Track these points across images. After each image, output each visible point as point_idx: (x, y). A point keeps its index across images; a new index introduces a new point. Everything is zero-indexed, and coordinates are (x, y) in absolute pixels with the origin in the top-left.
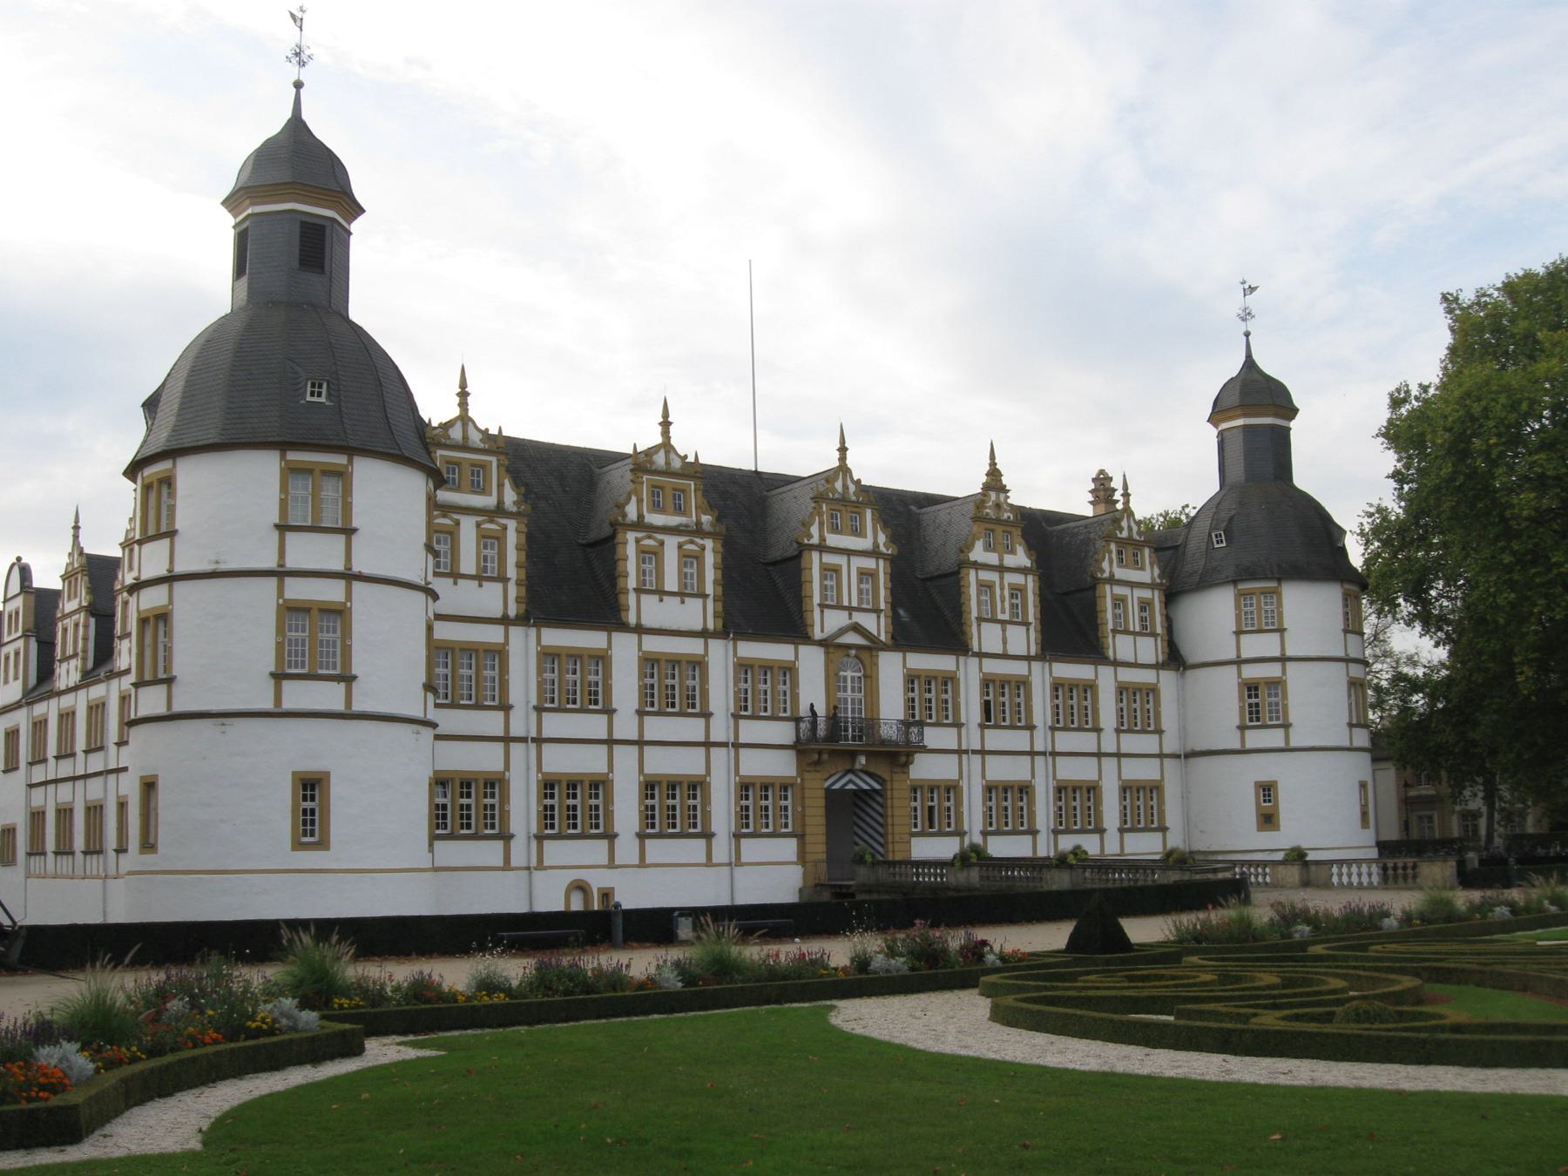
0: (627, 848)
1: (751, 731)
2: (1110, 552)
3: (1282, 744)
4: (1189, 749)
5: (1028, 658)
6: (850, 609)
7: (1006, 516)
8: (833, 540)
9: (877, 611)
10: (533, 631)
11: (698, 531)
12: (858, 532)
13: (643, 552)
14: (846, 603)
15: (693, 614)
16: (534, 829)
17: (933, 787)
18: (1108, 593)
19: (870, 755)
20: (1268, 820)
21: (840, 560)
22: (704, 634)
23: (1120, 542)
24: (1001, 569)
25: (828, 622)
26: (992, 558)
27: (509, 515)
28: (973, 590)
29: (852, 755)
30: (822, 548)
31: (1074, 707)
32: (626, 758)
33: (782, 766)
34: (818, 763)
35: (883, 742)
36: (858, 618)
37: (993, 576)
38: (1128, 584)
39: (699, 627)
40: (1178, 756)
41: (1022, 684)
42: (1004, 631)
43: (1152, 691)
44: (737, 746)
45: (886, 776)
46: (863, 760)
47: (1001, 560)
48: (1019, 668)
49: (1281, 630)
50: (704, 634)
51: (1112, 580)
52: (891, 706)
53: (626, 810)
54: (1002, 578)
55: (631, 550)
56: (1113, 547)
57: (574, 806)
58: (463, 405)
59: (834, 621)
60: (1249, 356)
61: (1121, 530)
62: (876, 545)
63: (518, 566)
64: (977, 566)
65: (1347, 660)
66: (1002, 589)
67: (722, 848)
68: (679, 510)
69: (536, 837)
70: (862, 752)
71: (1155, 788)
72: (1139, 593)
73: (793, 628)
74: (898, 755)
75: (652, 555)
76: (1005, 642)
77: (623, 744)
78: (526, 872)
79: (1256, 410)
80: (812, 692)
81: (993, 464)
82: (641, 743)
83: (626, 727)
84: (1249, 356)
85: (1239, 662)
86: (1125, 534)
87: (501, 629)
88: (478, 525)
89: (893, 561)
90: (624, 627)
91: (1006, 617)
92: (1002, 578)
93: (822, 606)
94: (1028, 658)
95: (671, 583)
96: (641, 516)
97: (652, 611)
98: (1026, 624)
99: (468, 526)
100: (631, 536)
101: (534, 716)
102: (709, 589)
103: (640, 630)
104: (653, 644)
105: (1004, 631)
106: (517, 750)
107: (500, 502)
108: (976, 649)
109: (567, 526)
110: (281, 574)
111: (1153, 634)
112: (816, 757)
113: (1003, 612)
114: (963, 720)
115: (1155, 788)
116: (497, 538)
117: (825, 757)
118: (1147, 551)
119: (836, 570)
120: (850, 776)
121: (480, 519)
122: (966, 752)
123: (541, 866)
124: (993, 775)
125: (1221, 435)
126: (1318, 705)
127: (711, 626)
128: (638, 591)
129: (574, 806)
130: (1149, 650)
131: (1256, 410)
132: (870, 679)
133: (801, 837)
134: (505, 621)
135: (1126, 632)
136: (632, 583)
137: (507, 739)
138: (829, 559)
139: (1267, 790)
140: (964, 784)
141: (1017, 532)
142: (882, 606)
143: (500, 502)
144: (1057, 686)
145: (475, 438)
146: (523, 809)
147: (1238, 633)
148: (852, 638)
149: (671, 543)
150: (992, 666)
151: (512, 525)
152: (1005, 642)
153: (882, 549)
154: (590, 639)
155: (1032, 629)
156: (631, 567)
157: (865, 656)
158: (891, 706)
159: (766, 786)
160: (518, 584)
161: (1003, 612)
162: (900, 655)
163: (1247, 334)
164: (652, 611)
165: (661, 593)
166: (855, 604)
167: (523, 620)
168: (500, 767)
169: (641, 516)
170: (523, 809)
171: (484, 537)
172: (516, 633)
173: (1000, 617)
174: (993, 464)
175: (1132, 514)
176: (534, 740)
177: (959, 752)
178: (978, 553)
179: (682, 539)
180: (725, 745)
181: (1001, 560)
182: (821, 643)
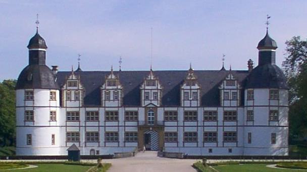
1: (128, 123)
2: (224, 83)
5: (197, 107)
8: (147, 88)
12: (154, 85)
15: (116, 104)
17: (171, 134)
20: (250, 141)
21: (149, 91)
23: (227, 80)
24: (191, 89)
25: (145, 103)
28: (182, 94)
31: (211, 117)
33: (135, 130)
35: (158, 125)
36: (153, 102)
37: (189, 91)
38: (229, 90)
39: (117, 106)
41: (196, 113)
43: (235, 113)
46: (151, 129)
48: (195, 109)
49: (253, 100)
52: (160, 117)
53: (102, 137)
55: (104, 93)
56: (225, 82)
59: (147, 102)
60: (267, 33)
61: (228, 77)
64: (184, 89)
65: (269, 106)
67: (200, 144)
68: (114, 85)
71: (235, 134)
72: (232, 91)
73: (138, 104)
74: (163, 127)
75: (108, 94)
77: (102, 126)
79: (266, 47)
80: (142, 117)
83: (102, 124)
84: (267, 33)
85: (247, 106)
86: (229, 79)
91: (192, 99)
95: (112, 99)
97: (108, 104)
98: (197, 100)
99: (73, 92)
100: (104, 91)
104: (107, 109)
110: (25, 107)
115: (235, 134)
118: (236, 82)
124: (186, 131)
125: (260, 53)
126: (261, 116)
128: (105, 100)
130: (234, 103)
131: (266, 47)
132: (156, 113)
133: (138, 142)
134: (79, 107)
136: (104, 99)
138: (146, 91)
139: (250, 134)
144: (205, 112)
147: (247, 100)
148: (152, 106)
150: (186, 109)
151: (81, 91)
153: (159, 88)
156: (104, 96)
158: (160, 117)
159: (132, 134)
161: (191, 97)
162: (163, 108)
163: (267, 28)
165: (109, 100)
166: (152, 99)
171: (76, 94)
178: (184, 86)
182: (143, 107)
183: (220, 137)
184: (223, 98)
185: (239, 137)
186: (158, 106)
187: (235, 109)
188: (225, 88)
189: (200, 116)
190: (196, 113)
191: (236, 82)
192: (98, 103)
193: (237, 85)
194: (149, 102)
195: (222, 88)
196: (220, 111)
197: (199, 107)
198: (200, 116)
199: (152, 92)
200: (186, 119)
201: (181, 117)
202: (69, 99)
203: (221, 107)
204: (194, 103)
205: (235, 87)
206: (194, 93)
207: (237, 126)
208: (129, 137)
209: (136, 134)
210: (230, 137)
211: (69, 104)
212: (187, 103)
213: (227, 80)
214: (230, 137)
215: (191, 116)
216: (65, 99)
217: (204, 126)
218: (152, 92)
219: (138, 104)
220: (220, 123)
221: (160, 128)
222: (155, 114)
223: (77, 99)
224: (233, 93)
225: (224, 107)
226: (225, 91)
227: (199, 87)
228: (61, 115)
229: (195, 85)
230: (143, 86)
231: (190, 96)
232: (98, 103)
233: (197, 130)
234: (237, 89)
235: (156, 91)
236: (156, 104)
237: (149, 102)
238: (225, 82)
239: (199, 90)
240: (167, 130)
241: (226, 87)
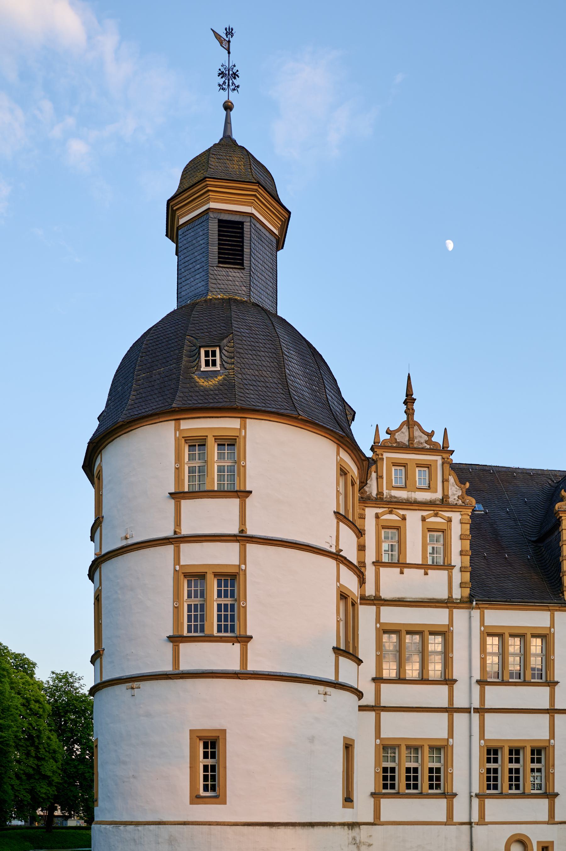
10: (476, 613)
16: (476, 790)
27: (454, 507)
58: (410, 412)
63: (462, 553)
69: (477, 795)
78: (468, 827)
88: (424, 519)
99: (414, 519)
101: (476, 689)
106: (460, 719)
107: (445, 497)
116: (443, 531)
121: (425, 513)
137: (450, 710)
143: (445, 497)
145: (421, 439)
146: (466, 772)
160: (462, 570)
167: (466, 603)
168: (444, 735)
170: (466, 772)
172: (460, 615)
176: (476, 710)
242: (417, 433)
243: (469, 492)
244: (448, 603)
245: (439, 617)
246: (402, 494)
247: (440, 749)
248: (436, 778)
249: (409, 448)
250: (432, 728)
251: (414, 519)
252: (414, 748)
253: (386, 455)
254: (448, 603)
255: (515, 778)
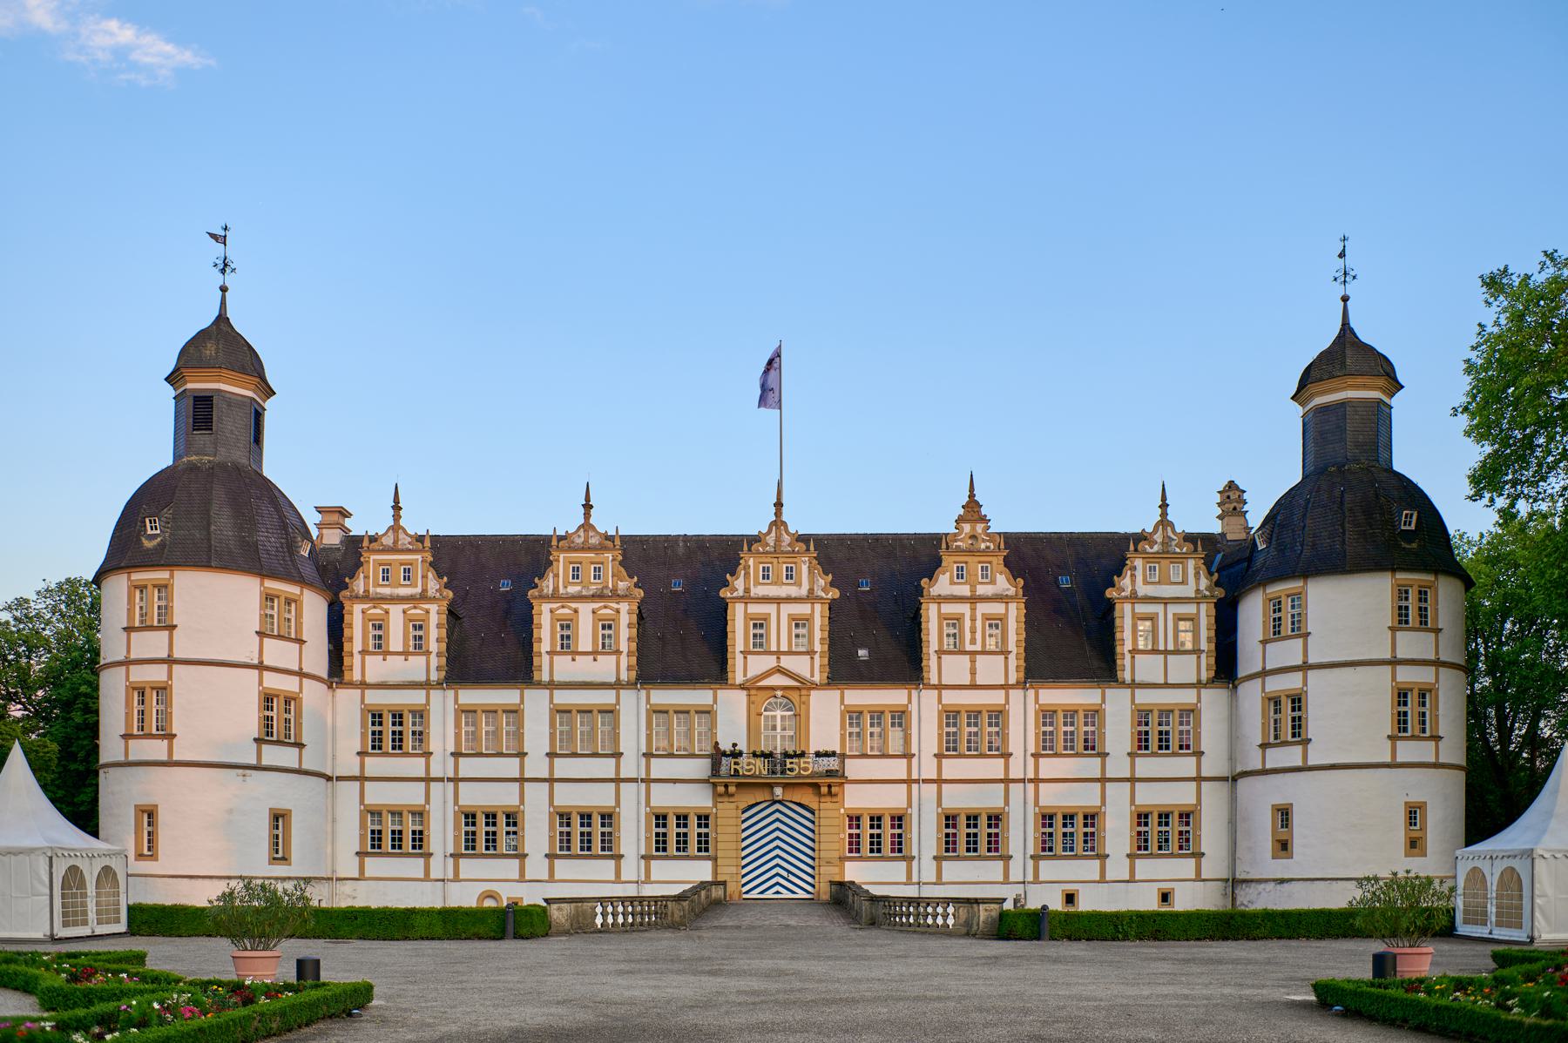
0: (537, 866)
3: (1299, 763)
4: (1239, 770)
5: (1005, 687)
6: (778, 653)
7: (983, 546)
9: (811, 653)
10: (451, 693)
11: (616, 596)
13: (555, 618)
14: (774, 648)
16: (451, 850)
18: (1125, 615)
19: (785, 786)
21: (770, 609)
22: (617, 685)
25: (745, 665)
26: (965, 590)
27: (433, 600)
29: (770, 786)
30: (747, 599)
32: (537, 796)
33: (698, 799)
34: (727, 794)
36: (787, 662)
37: (965, 609)
39: (613, 680)
40: (1225, 779)
42: (973, 662)
44: (648, 781)
45: (814, 806)
46: (778, 791)
47: (973, 590)
48: (996, 698)
50: (617, 685)
51: (1134, 598)
53: (537, 834)
54: (973, 610)
56: (1139, 563)
57: (488, 832)
61: (1153, 543)
62: (811, 591)
64: (941, 599)
66: (973, 620)
70: (778, 784)
72: (1173, 609)
76: (973, 673)
81: (972, 496)
82: (551, 780)
86: (1156, 548)
87: (423, 693)
89: (833, 606)
90: (540, 685)
91: (978, 647)
92: (973, 610)
93: (745, 653)
94: (1005, 687)
96: (556, 589)
97: (565, 668)
99: (396, 613)
102: (624, 647)
103: (552, 685)
104: (564, 698)
105: (973, 662)
107: (424, 590)
108: (934, 681)
109: (491, 602)
111: (1197, 651)
112: (721, 789)
113: (973, 641)
114: (914, 750)
117: (732, 789)
118: (1191, 564)
119: (766, 618)
120: (777, 806)
122: (917, 781)
123: (456, 879)
127: (624, 676)
129: (488, 832)
130: (1186, 669)
133: (715, 859)
135: (1155, 651)
137: (428, 780)
138: (754, 609)
140: (914, 811)
141: (998, 562)
142: (817, 647)
143: (424, 590)
145: (404, 541)
149: (585, 609)
150: (951, 698)
152: (973, 673)
154: (504, 696)
155: (1012, 657)
157: (794, 696)
160: (439, 655)
161: (973, 641)
162: (835, 694)
164: (565, 668)
166: (784, 648)
169: (556, 589)
171: (408, 619)
172: (436, 695)
173: (968, 647)
174: (972, 496)
175: (1171, 524)
177: (909, 782)
178: (943, 584)
179: (596, 605)
180: (634, 780)
181: (973, 590)
182: (742, 687)
183: (1117, 833)
184: (1128, 646)
185: (1211, 835)
186: (817, 679)
187: (1187, 697)
188: (1140, 594)
189: (1021, 732)
190: (998, 715)
191: (1191, 564)
192: (517, 667)
193: (1197, 575)
194: (769, 662)
195: (1127, 593)
196: (1118, 707)
197: (1013, 687)
198: (1021, 732)
199: (779, 621)
200: (950, 748)
201: (927, 734)
202: (380, 646)
203: (1123, 684)
204: (991, 669)
205: (1189, 591)
206: (986, 617)
207: (1199, 779)
208: (672, 834)
209: (704, 819)
210: (1163, 832)
211: (376, 668)
212: (954, 669)
213: (1149, 558)
214: (1163, 832)
215: (972, 732)
216: (357, 645)
217: (1036, 781)
218: (779, 621)
219: (715, 670)
220: (1118, 765)
221: (824, 790)
222: (800, 719)
223: (419, 646)
224: (1179, 618)
225: (1134, 685)
226: (1141, 609)
227: (1012, 591)
228: (335, 721)
229: (993, 582)
230: (739, 584)
231: (968, 636)
232: (517, 667)
233: (1007, 802)
234: (1198, 599)
235: (804, 609)
236: (806, 674)
237: (769, 662)
238: (1139, 563)
239: (1013, 607)
240: (856, 798)
241: (1142, 590)
242: (402, 535)
243: (447, 586)
244: (426, 685)
245: (416, 698)
246: (387, 591)
247: (420, 814)
248: (419, 838)
249: (394, 550)
250: (411, 795)
251: (396, 613)
252: (397, 813)
253: (373, 557)
254: (426, 685)
255: (491, 839)
